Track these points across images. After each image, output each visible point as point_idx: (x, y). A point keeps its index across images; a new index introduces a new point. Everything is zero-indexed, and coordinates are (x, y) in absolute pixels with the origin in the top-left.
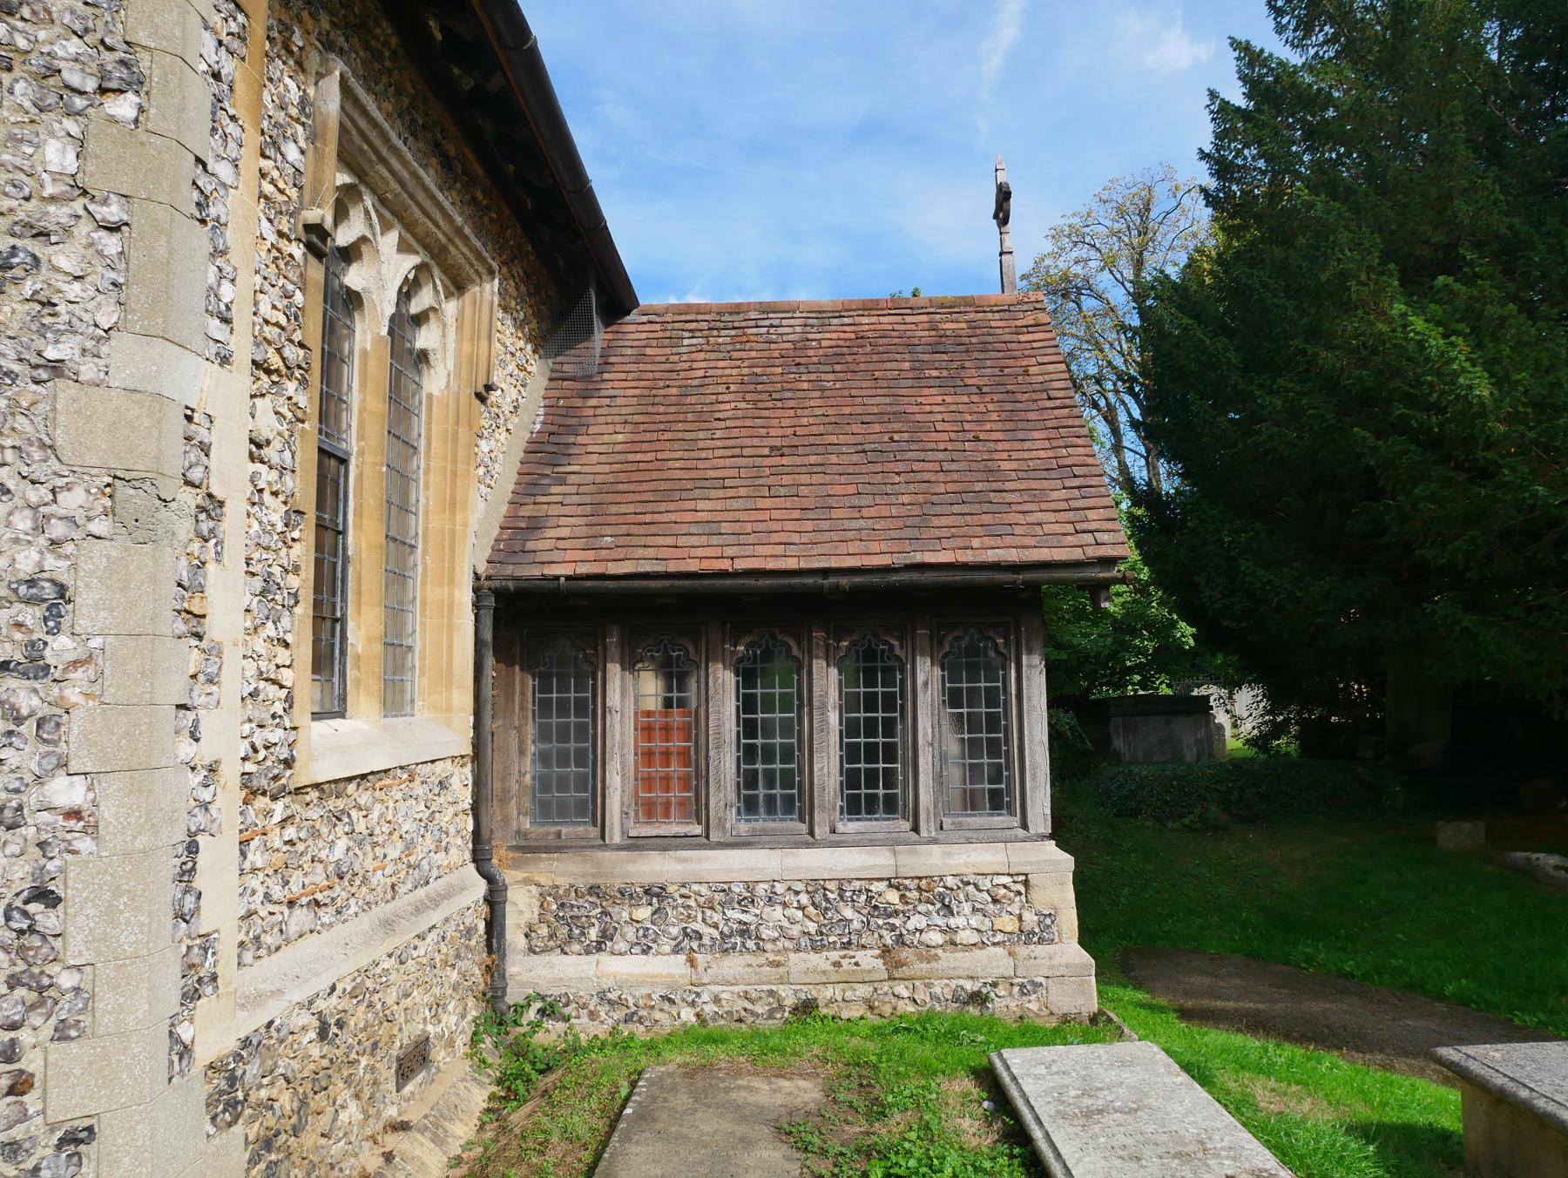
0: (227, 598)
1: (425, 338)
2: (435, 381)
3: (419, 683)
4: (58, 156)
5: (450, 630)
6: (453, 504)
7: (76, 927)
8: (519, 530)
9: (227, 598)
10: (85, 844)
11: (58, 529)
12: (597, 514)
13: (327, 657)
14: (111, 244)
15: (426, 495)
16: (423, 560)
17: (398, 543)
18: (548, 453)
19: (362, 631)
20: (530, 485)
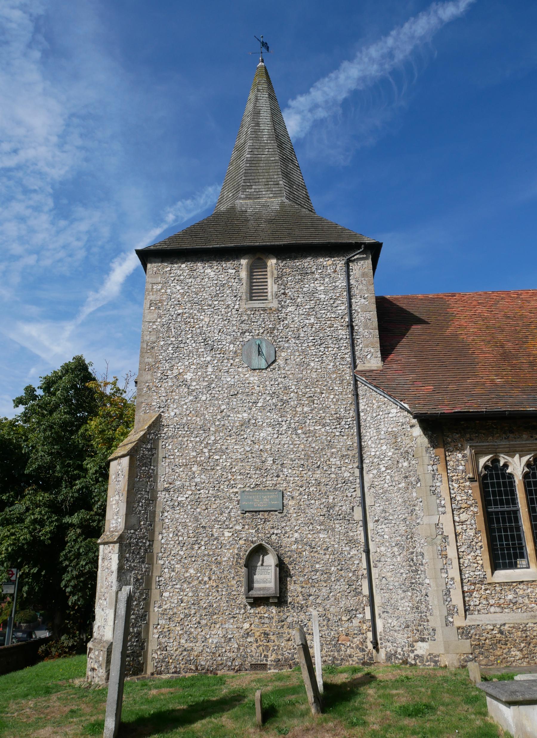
4: (414, 494)
10: (430, 588)
11: (422, 545)
14: (421, 504)
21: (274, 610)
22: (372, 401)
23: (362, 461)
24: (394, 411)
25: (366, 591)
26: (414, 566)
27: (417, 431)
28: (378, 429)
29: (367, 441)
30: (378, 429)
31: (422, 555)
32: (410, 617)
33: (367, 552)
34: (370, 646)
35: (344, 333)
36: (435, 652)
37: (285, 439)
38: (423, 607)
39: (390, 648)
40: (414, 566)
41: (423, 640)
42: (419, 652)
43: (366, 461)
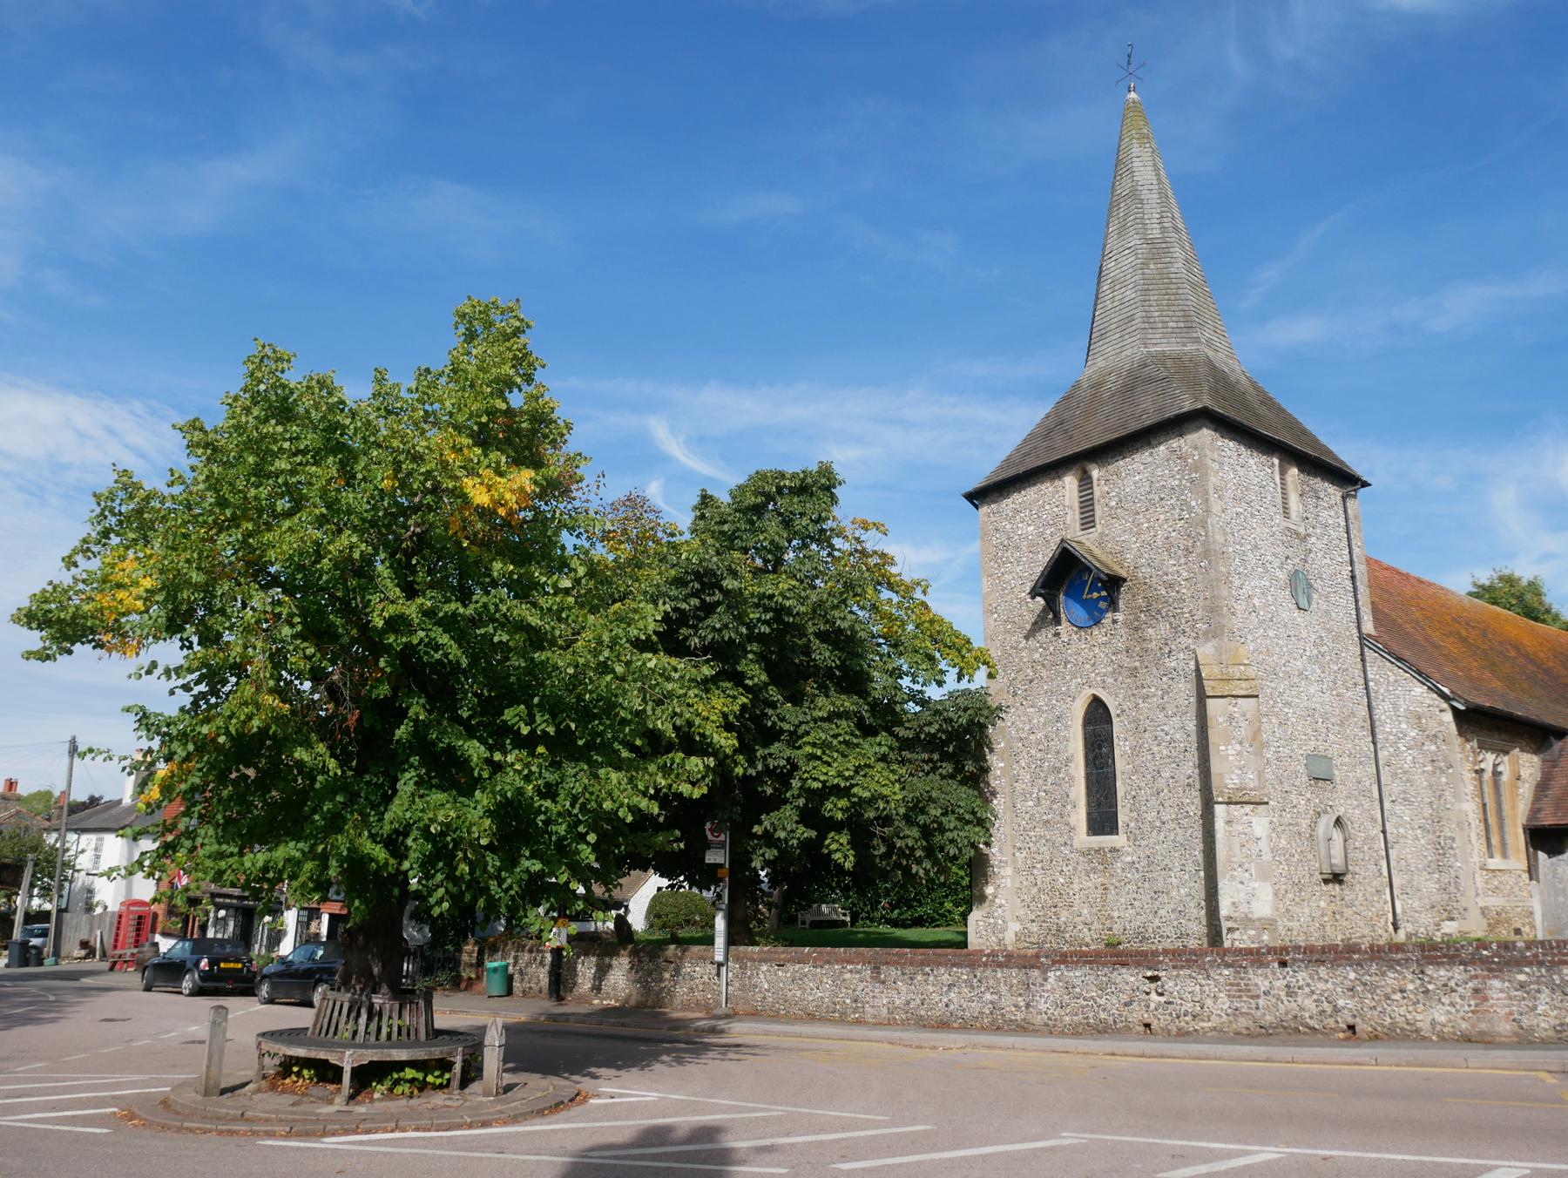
0: (1474, 838)
1: (1500, 769)
2: (1505, 778)
3: (1510, 852)
5: (1518, 839)
6: (1514, 807)
7: (1462, 881)
8: (1534, 812)
9: (1474, 838)
12: (1557, 807)
13: (1489, 845)
15: (1506, 806)
16: (1508, 822)
17: (1501, 819)
18: (1542, 788)
19: (1495, 840)
20: (1537, 798)
21: (1337, 887)
22: (1384, 673)
23: (1373, 734)
24: (1419, 690)
25: (1385, 873)
26: (1442, 850)
27: (1448, 717)
28: (1395, 706)
29: (1379, 713)
30: (1395, 706)
31: (1453, 839)
32: (1436, 898)
33: (1384, 832)
34: (1391, 928)
35: (1348, 583)
36: (1466, 929)
37: (1327, 697)
38: (1452, 889)
39: (1410, 929)
40: (1442, 850)
41: (1452, 919)
42: (1448, 931)
43: (1380, 736)
